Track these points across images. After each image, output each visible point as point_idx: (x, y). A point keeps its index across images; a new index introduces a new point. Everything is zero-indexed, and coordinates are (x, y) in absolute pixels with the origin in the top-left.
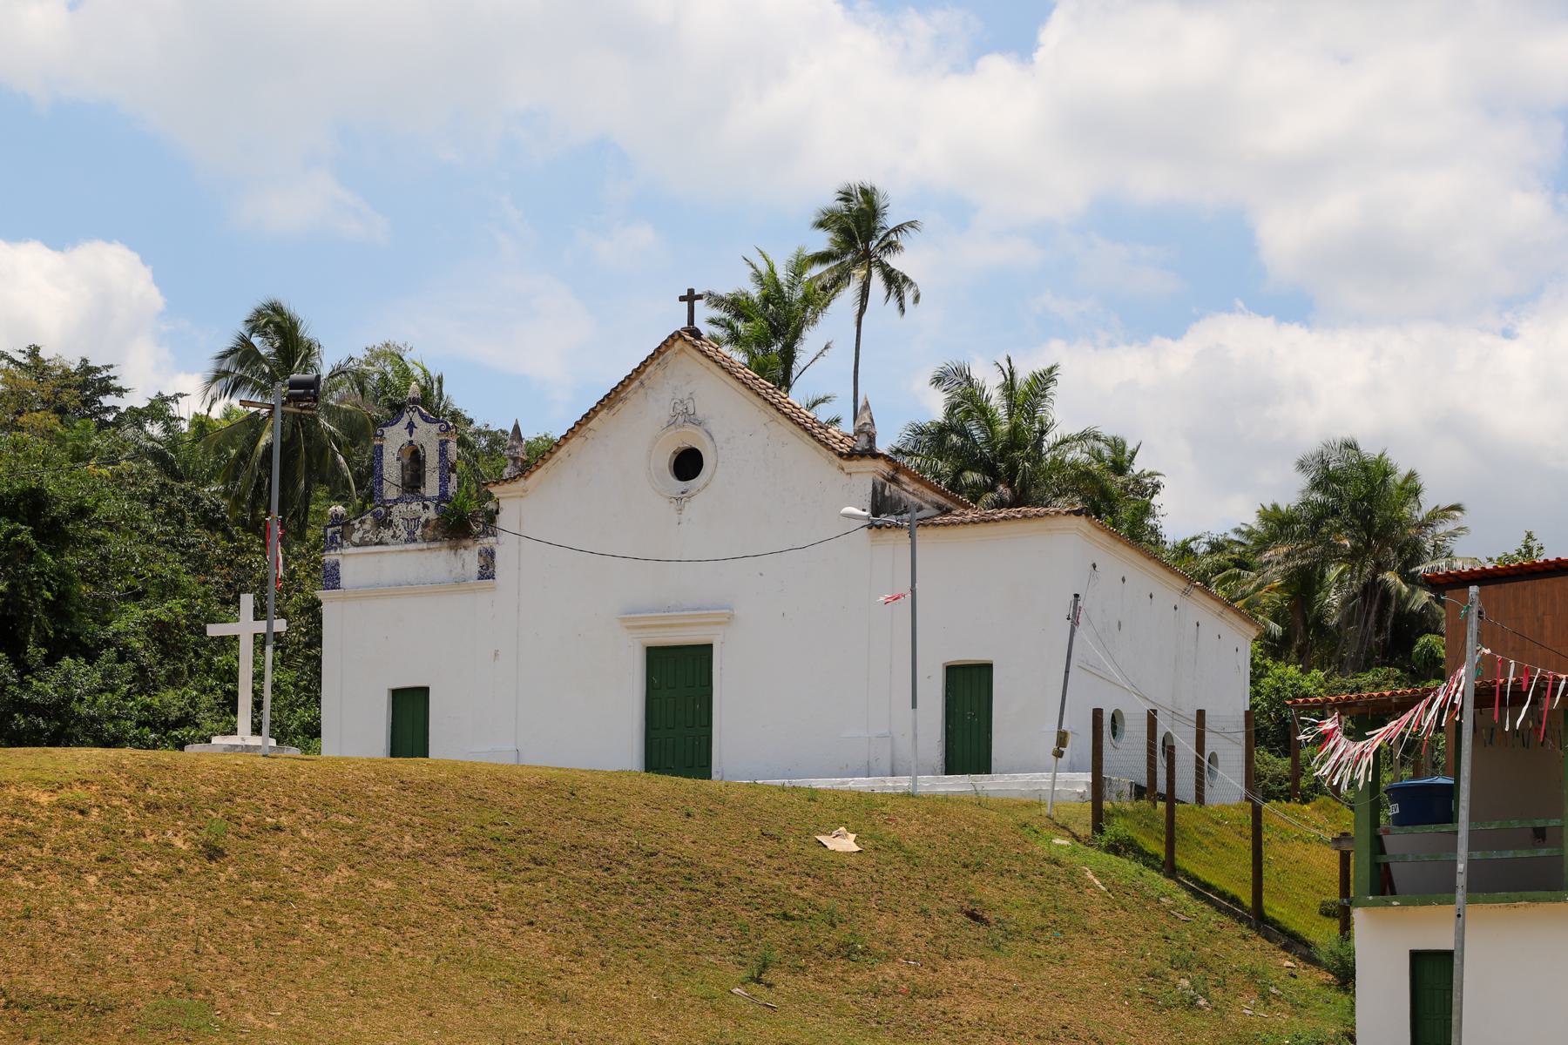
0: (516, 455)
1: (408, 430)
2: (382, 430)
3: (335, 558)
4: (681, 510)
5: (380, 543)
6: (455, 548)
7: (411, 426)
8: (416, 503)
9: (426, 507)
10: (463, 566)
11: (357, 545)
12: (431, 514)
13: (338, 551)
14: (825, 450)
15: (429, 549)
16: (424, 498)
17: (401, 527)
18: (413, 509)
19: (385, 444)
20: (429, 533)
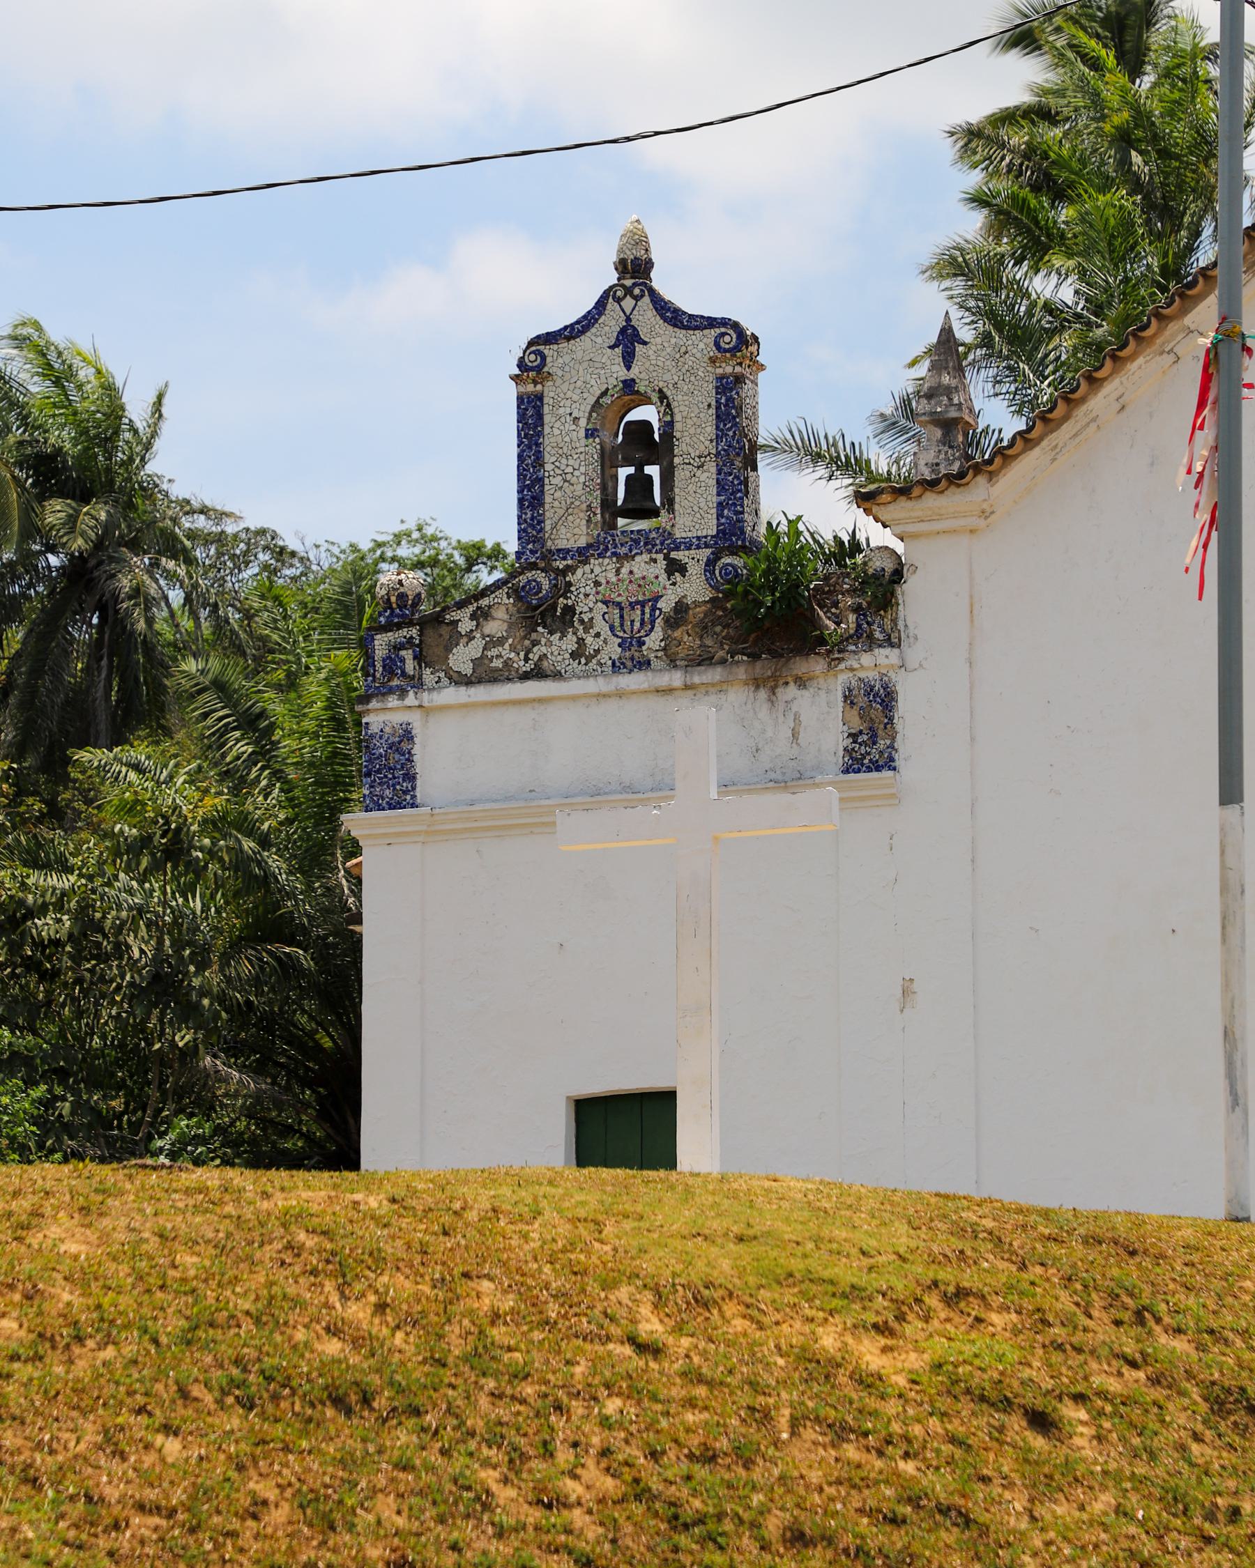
0: (953, 414)
1: (618, 351)
2: (536, 353)
3: (397, 718)
5: (537, 674)
6: (769, 684)
7: (628, 340)
8: (646, 557)
9: (675, 568)
10: (795, 735)
11: (467, 681)
13: (411, 699)
15: (687, 687)
17: (601, 626)
18: (638, 574)
19: (549, 391)
20: (687, 639)
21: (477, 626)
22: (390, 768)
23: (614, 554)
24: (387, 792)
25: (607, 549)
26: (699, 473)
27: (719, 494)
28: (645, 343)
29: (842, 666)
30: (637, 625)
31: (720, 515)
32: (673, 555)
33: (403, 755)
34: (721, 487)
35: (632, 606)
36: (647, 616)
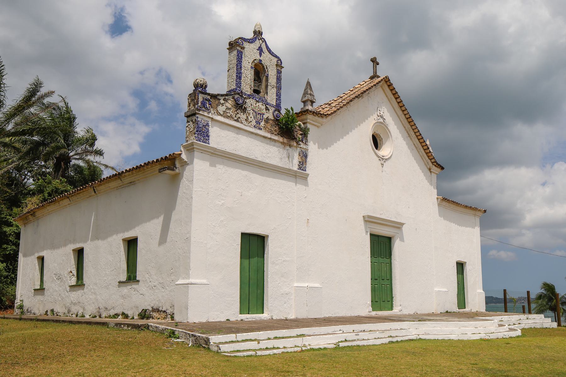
2: (242, 42)
5: (237, 121)
8: (261, 103)
9: (267, 109)
12: (269, 115)
14: (427, 158)
16: (266, 104)
17: (251, 115)
20: (269, 126)
21: (225, 103)
22: (203, 132)
23: (255, 99)
24: (202, 138)
25: (254, 97)
26: (272, 89)
27: (276, 96)
28: (264, 53)
29: (299, 146)
30: (259, 119)
31: (276, 101)
32: (267, 106)
33: (206, 129)
34: (277, 95)
35: (259, 114)
36: (261, 118)
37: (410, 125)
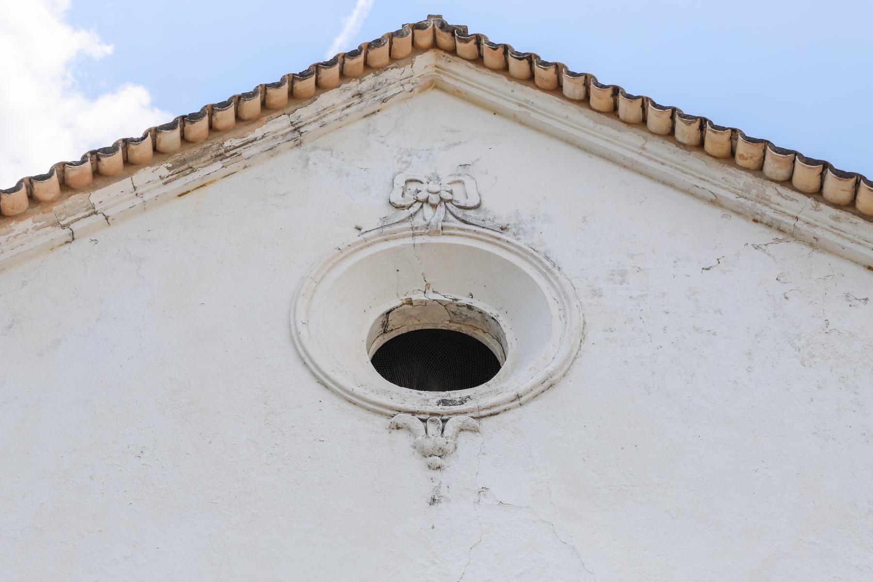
4: (442, 453)
37: (747, 169)
